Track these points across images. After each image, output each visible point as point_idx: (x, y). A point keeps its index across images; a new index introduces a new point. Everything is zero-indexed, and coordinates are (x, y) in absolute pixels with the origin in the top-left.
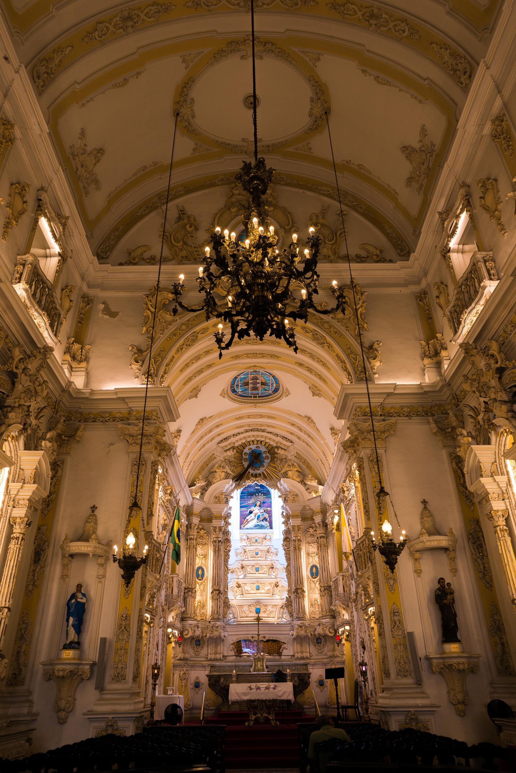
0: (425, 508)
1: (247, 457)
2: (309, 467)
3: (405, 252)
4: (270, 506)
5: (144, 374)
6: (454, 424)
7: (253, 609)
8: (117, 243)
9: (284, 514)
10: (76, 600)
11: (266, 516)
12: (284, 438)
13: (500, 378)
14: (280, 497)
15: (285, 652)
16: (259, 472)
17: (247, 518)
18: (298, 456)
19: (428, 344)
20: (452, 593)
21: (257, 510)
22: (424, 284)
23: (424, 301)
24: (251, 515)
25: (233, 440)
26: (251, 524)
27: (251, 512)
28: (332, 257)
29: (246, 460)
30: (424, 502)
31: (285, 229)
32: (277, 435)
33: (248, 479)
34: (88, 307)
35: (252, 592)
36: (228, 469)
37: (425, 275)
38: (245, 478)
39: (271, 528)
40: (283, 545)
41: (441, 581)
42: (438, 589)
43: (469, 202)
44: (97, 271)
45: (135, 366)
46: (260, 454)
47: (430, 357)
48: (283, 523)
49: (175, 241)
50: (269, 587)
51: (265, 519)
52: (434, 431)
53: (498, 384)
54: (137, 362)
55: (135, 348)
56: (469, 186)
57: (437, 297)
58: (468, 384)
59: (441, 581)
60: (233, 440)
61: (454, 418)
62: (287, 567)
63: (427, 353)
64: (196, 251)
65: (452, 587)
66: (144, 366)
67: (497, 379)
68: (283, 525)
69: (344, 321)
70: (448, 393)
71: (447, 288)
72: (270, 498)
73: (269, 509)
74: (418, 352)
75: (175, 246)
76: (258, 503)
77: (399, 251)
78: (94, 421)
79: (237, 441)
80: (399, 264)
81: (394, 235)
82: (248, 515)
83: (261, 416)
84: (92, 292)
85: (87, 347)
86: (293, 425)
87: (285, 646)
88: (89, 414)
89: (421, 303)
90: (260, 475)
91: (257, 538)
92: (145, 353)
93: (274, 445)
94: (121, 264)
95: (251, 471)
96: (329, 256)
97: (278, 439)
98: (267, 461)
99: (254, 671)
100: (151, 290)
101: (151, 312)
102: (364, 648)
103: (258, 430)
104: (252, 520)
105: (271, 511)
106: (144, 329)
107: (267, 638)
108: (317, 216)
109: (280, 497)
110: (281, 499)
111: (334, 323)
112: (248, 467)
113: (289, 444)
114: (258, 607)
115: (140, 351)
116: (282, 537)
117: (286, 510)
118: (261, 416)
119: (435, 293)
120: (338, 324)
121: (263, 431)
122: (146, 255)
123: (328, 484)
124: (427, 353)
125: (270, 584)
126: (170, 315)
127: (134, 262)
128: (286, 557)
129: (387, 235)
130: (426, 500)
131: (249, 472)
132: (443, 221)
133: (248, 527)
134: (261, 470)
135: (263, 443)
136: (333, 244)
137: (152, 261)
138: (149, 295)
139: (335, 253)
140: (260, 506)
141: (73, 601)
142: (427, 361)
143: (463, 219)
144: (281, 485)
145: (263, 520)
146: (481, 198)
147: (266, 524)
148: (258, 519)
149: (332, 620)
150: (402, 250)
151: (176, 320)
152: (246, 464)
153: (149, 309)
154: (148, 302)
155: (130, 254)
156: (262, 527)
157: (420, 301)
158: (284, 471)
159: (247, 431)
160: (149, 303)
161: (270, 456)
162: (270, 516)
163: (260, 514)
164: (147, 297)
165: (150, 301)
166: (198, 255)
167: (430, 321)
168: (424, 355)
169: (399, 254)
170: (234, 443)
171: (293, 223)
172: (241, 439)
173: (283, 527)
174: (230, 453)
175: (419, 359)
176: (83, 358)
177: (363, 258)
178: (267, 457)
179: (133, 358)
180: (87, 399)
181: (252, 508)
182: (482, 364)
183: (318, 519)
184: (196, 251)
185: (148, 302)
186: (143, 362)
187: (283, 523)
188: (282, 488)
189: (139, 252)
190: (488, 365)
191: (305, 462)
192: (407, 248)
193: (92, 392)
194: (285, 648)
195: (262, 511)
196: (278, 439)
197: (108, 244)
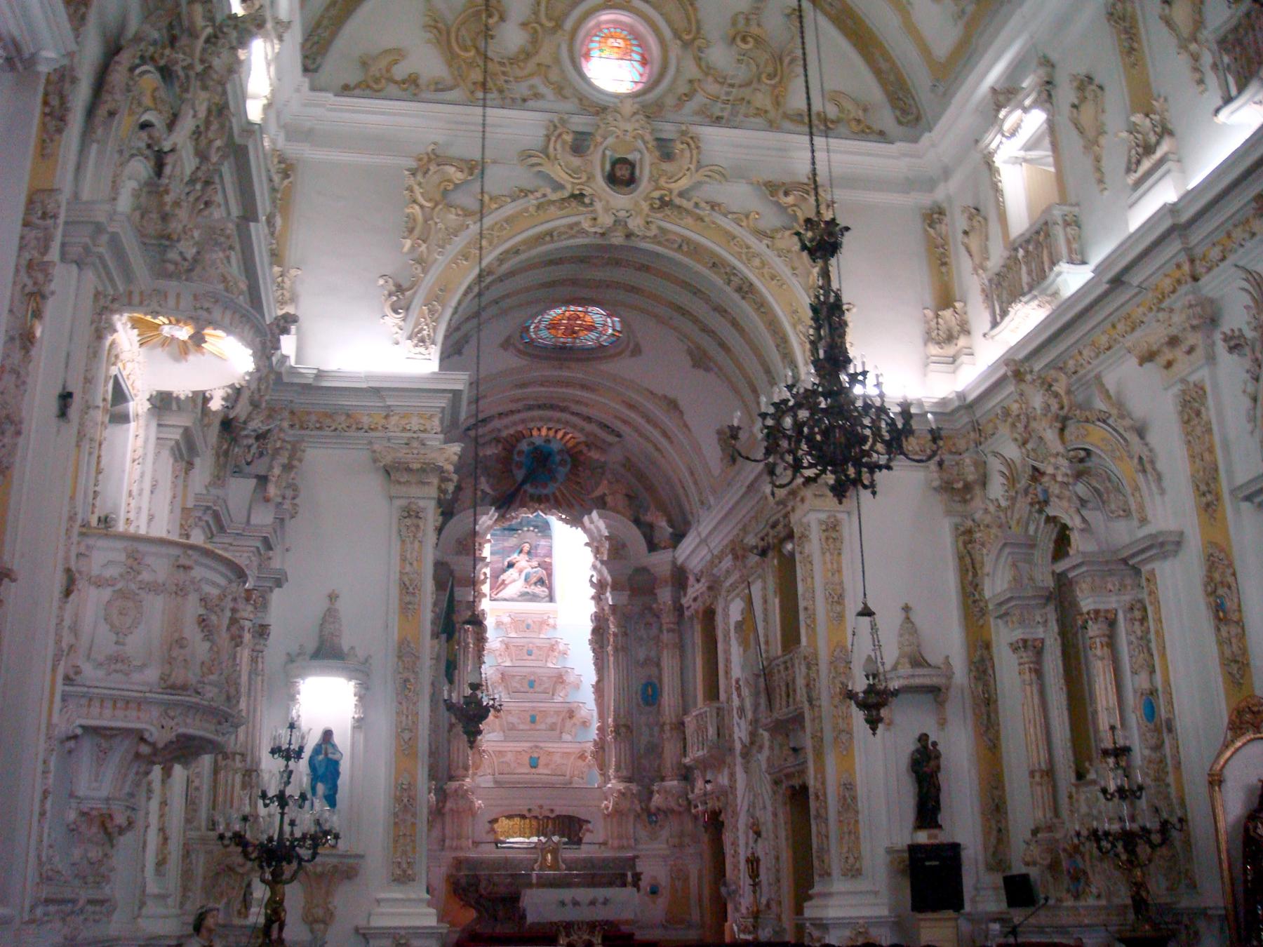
0: (908, 618)
1: (523, 459)
2: (650, 488)
3: (910, 117)
4: (549, 555)
5: (410, 338)
6: (971, 478)
7: (526, 760)
8: (334, 34)
9: (594, 580)
10: (326, 754)
11: (542, 573)
12: (604, 426)
13: (1062, 430)
14: (587, 544)
15: (587, 838)
16: (545, 492)
17: (502, 577)
18: (628, 464)
19: (937, 316)
20: (938, 756)
21: (522, 561)
22: (940, 195)
23: (938, 226)
24: (511, 571)
25: (496, 424)
26: (511, 591)
27: (511, 565)
28: (772, 114)
29: (519, 465)
30: (906, 609)
31: (680, 38)
32: (588, 419)
33: (523, 505)
34: (286, 182)
35: (521, 727)
36: (484, 485)
37: (946, 173)
38: (517, 503)
39: (551, 598)
40: (591, 642)
41: (923, 738)
42: (918, 751)
43: (1050, 96)
44: (305, 105)
45: (392, 320)
46: (550, 454)
47: (938, 343)
48: (593, 598)
49: (460, 47)
50: (554, 720)
51: (541, 582)
52: (936, 483)
53: (1057, 438)
54: (396, 311)
55: (390, 281)
56: (1053, 66)
57: (966, 233)
58: (1008, 424)
59: (923, 738)
60: (496, 424)
61: (972, 468)
62: (598, 682)
63: (934, 334)
64: (504, 73)
65: (939, 747)
66: (409, 319)
67: (1057, 431)
68: (592, 603)
69: (789, 255)
70: (965, 419)
71: (987, 224)
72: (549, 537)
73: (547, 560)
74: (915, 331)
75: (458, 56)
76: (526, 547)
77: (898, 113)
78: (320, 428)
79: (506, 427)
80: (899, 146)
81: (892, 78)
82: (504, 571)
83: (567, 384)
84: (294, 150)
85: (293, 272)
86: (631, 406)
87: (590, 826)
88: (309, 413)
89: (931, 231)
90: (546, 496)
91: (530, 621)
92: (408, 293)
93: (581, 438)
94: (346, 90)
95: (528, 488)
96: (766, 112)
97: (589, 427)
98: (563, 471)
99: (541, 869)
100: (420, 160)
101: (422, 207)
102: (758, 834)
103: (553, 407)
104: (514, 581)
105: (550, 564)
106: (408, 243)
107: (557, 813)
108: (748, 19)
109: (587, 544)
110: (589, 549)
111: (770, 256)
112: (524, 482)
113: (611, 439)
114: (535, 755)
115: (400, 289)
116: (588, 626)
117: (599, 572)
118: (567, 384)
119: (961, 223)
120: (777, 259)
121: (563, 410)
122: (400, 71)
123: (699, 534)
124: (934, 334)
125: (558, 713)
126: (458, 215)
127: (375, 87)
128: (596, 664)
129: (878, 72)
130: (910, 604)
131: (525, 492)
132: (999, 107)
133: (506, 596)
134: (551, 489)
135: (560, 434)
136: (774, 87)
137: (412, 87)
138: (417, 170)
139: (777, 103)
140: (529, 553)
141: (321, 757)
142: (934, 350)
143: (1035, 120)
144: (592, 522)
145: (535, 584)
146: (1074, 106)
147: (540, 590)
148: (526, 580)
149: (683, 784)
150: (904, 112)
151: (468, 227)
152: (520, 475)
153: (415, 201)
154: (416, 188)
155: (364, 64)
156: (533, 598)
157: (930, 226)
158: (597, 493)
159: (530, 408)
160: (418, 190)
161: (569, 459)
162: (550, 575)
163: (529, 570)
164: (413, 174)
165: (420, 184)
166: (506, 81)
167: (944, 269)
168: (929, 338)
169: (897, 118)
170: (499, 430)
171: (699, 29)
172: (515, 424)
173: (591, 608)
174: (490, 451)
175: (918, 340)
176: (287, 295)
177: (832, 122)
178: (563, 463)
179: (389, 303)
180: (306, 388)
181: (514, 557)
182: (1038, 400)
183: (665, 595)
184: (504, 73)
185: (416, 188)
186: (407, 309)
187: (593, 598)
188: (592, 526)
189: (383, 63)
190: (1047, 407)
191: (641, 477)
192: (914, 110)
193: (320, 374)
194: (588, 830)
195: (535, 563)
196: (589, 427)
197: (316, 38)
